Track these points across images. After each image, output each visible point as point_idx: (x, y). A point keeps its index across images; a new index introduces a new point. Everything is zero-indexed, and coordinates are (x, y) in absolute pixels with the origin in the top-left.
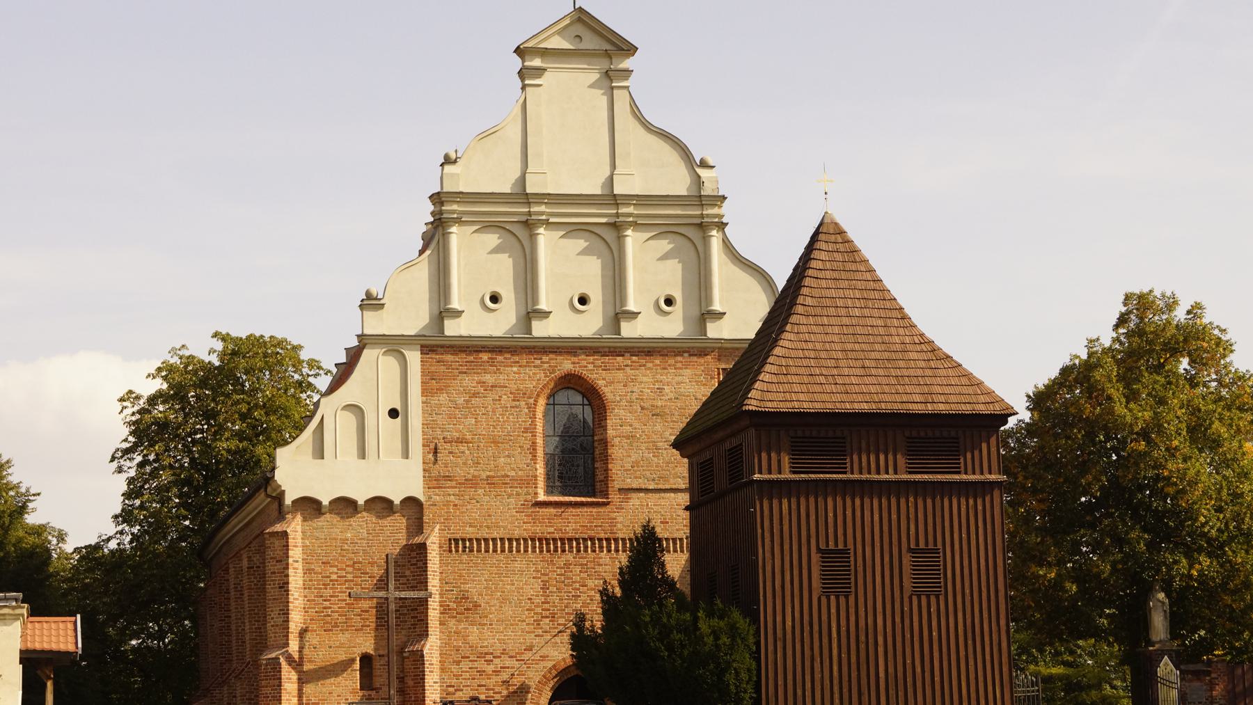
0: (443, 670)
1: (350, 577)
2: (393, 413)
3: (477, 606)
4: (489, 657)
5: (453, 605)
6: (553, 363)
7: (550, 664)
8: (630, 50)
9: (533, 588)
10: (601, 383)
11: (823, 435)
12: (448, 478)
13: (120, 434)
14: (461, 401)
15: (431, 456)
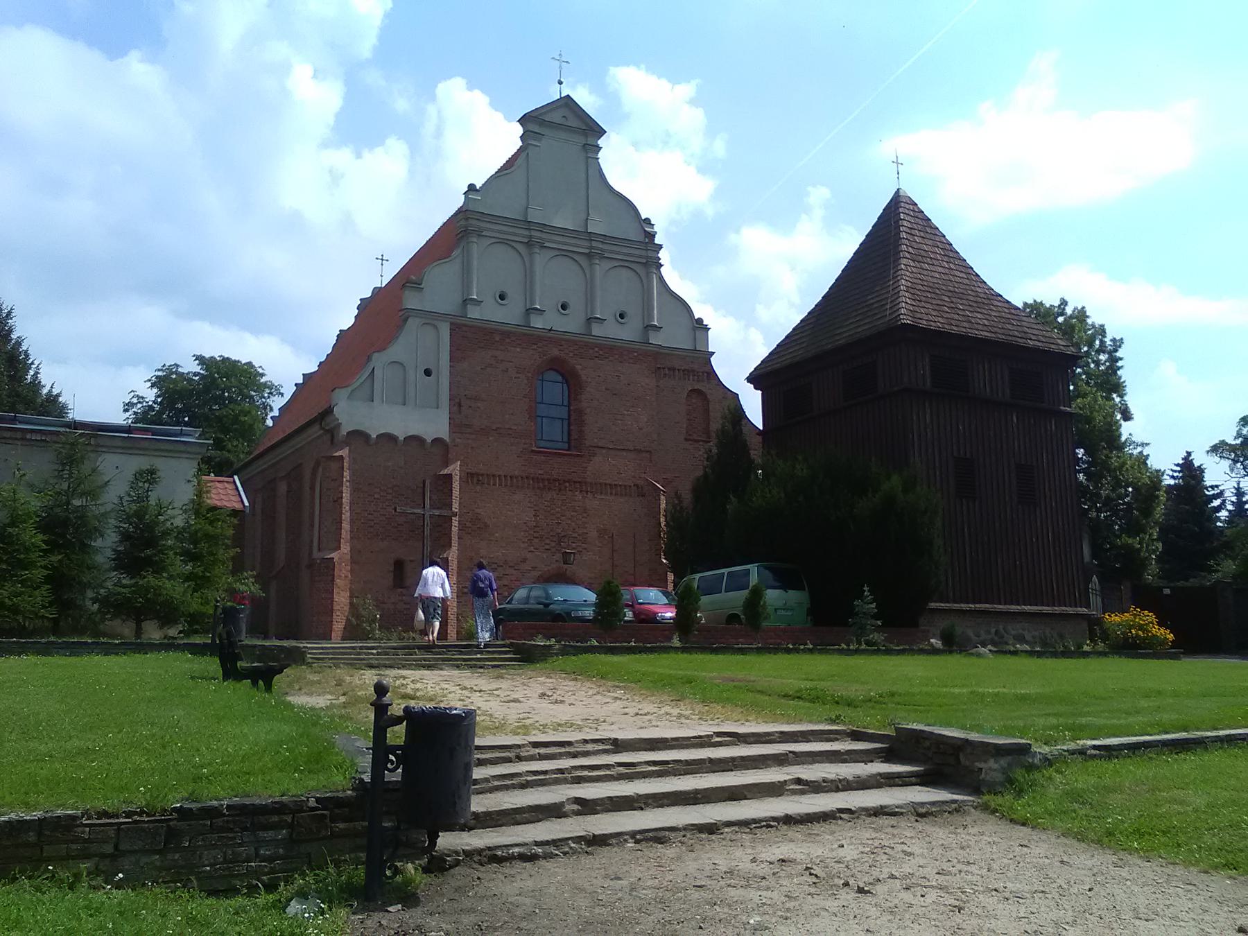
1: (389, 497)
2: (428, 373)
3: (486, 526)
5: (468, 524)
10: (578, 367)
15: (456, 408)
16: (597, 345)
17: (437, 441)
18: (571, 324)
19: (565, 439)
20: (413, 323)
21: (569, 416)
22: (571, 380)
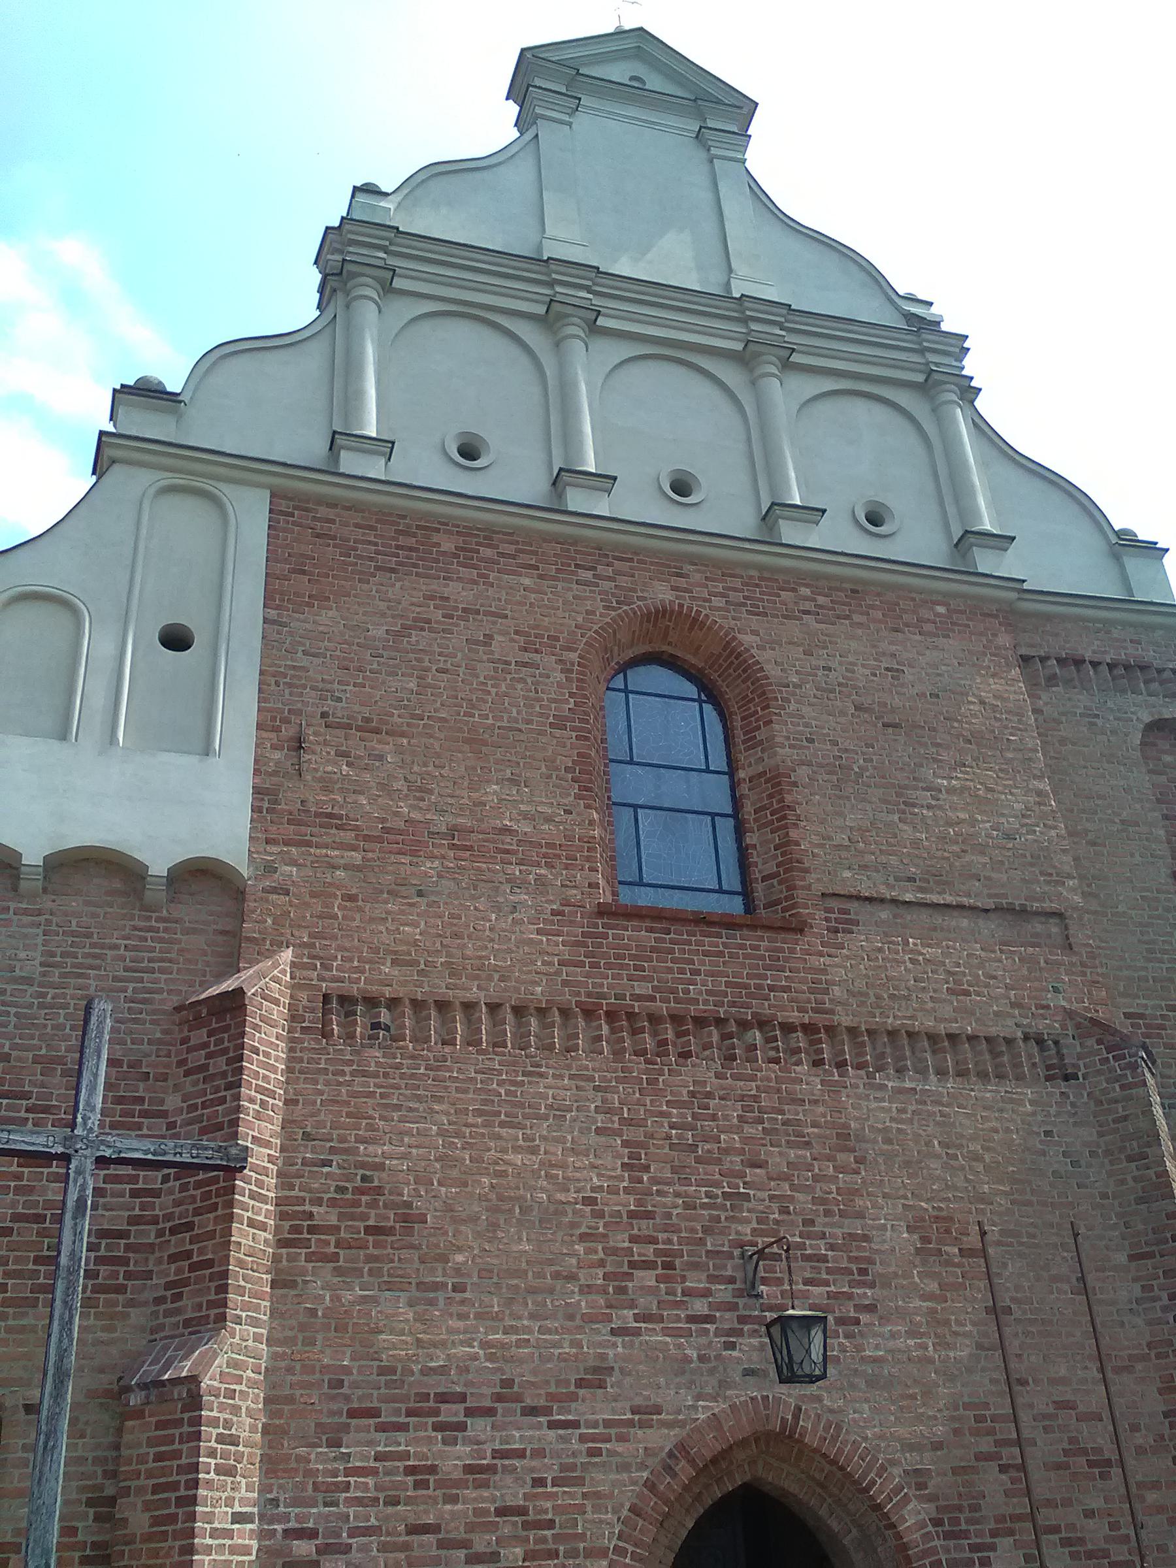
0: (272, 1465)
3: (409, 1219)
4: (452, 1413)
5: (324, 1215)
6: (624, 581)
7: (662, 1439)
9: (597, 1170)
10: (747, 639)
12: (330, 819)
14: (378, 632)
16: (802, 578)
17: (199, 875)
19: (732, 880)
21: (736, 802)
22: (723, 683)
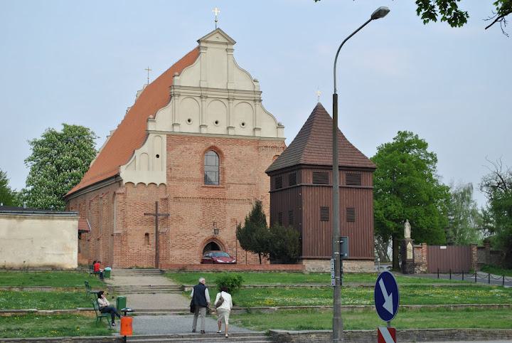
2: (158, 156)
8: (234, 43)
9: (200, 213)
10: (222, 149)
11: (322, 172)
13: (30, 153)
18: (220, 130)
20: (151, 136)
22: (219, 153)
